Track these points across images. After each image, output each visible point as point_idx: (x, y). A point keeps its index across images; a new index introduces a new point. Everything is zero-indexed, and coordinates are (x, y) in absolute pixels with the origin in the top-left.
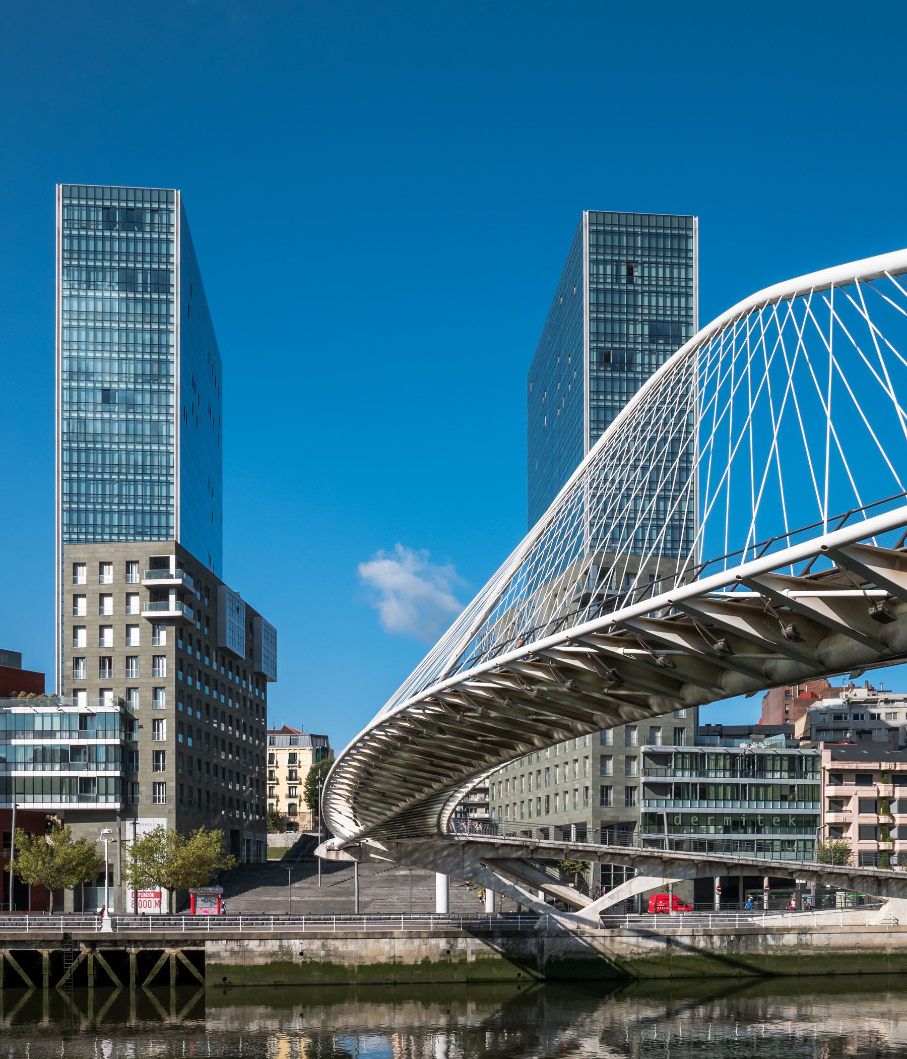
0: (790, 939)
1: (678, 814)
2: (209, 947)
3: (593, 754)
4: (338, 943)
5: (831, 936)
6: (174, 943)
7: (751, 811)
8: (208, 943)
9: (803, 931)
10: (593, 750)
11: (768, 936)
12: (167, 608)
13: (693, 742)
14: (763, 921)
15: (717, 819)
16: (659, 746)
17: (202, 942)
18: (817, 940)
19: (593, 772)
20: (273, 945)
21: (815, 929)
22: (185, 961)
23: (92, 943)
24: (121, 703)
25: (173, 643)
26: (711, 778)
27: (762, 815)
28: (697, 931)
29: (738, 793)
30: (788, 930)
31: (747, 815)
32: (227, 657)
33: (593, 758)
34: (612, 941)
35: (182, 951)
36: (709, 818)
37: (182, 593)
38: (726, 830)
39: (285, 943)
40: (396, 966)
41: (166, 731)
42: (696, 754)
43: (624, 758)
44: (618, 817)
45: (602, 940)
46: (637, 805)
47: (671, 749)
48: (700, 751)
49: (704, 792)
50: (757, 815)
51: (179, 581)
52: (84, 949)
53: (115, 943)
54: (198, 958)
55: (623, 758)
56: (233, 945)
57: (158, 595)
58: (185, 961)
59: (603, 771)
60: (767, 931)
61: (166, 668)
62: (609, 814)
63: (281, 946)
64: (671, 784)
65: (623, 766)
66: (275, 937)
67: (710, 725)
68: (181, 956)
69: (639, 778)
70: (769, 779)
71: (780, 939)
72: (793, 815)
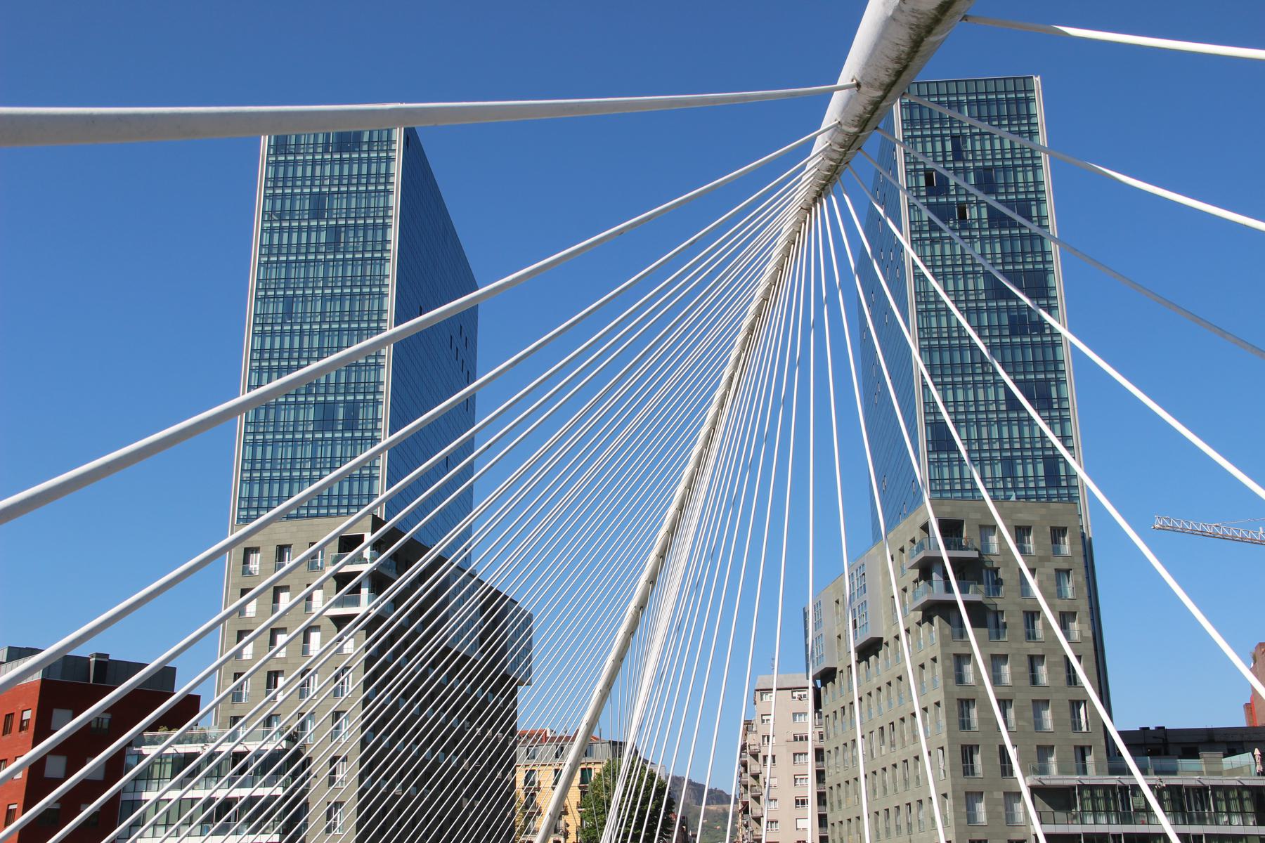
3: (953, 792)
10: (953, 786)
13: (1107, 769)
16: (1055, 776)
19: (955, 819)
33: (954, 798)
41: (348, 774)
42: (1113, 787)
43: (1002, 796)
47: (1073, 780)
48: (1118, 783)
55: (999, 795)
59: (971, 817)
64: (1079, 836)
65: (1002, 809)
67: (1148, 728)
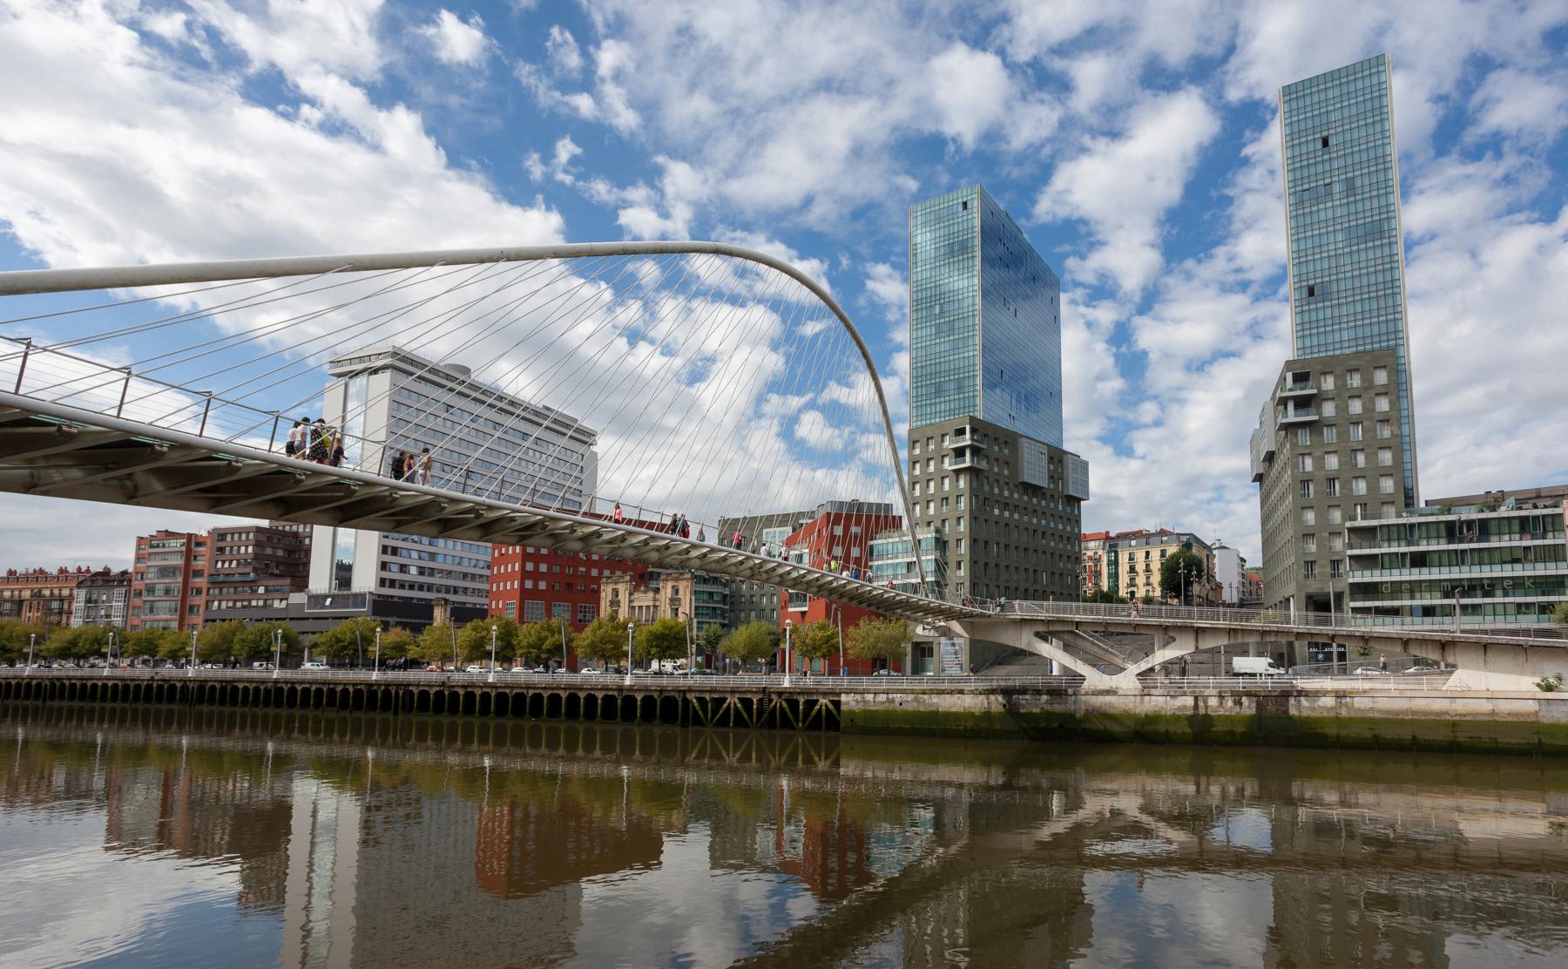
0: (1329, 701)
1: (1387, 582)
2: (844, 698)
4: (926, 697)
5: (1376, 699)
6: (825, 694)
7: (1474, 575)
8: (843, 695)
9: (1340, 695)
11: (1302, 699)
12: (964, 462)
14: (1302, 683)
15: (1432, 585)
17: (839, 694)
18: (1360, 703)
20: (882, 697)
21: (1357, 692)
22: (831, 707)
23: (780, 694)
24: (937, 531)
25: (968, 485)
26: (1423, 547)
27: (1488, 579)
28: (1225, 692)
29: (1459, 558)
30: (1325, 693)
31: (1470, 580)
32: (1030, 489)
34: (1142, 701)
35: (831, 701)
36: (1423, 585)
37: (976, 451)
38: (1446, 595)
39: (890, 696)
40: (969, 715)
41: (964, 549)
44: (1323, 589)
45: (1133, 698)
46: (1344, 577)
49: (1420, 560)
50: (1482, 579)
51: (969, 442)
52: (774, 697)
53: (791, 693)
54: (837, 704)
56: (858, 697)
57: (960, 453)
58: (831, 707)
60: (1302, 693)
61: (963, 504)
62: (1314, 586)
63: (888, 698)
66: (887, 692)
68: (829, 703)
69: (1344, 552)
70: (1494, 544)
71: (1315, 701)
72: (1529, 577)
